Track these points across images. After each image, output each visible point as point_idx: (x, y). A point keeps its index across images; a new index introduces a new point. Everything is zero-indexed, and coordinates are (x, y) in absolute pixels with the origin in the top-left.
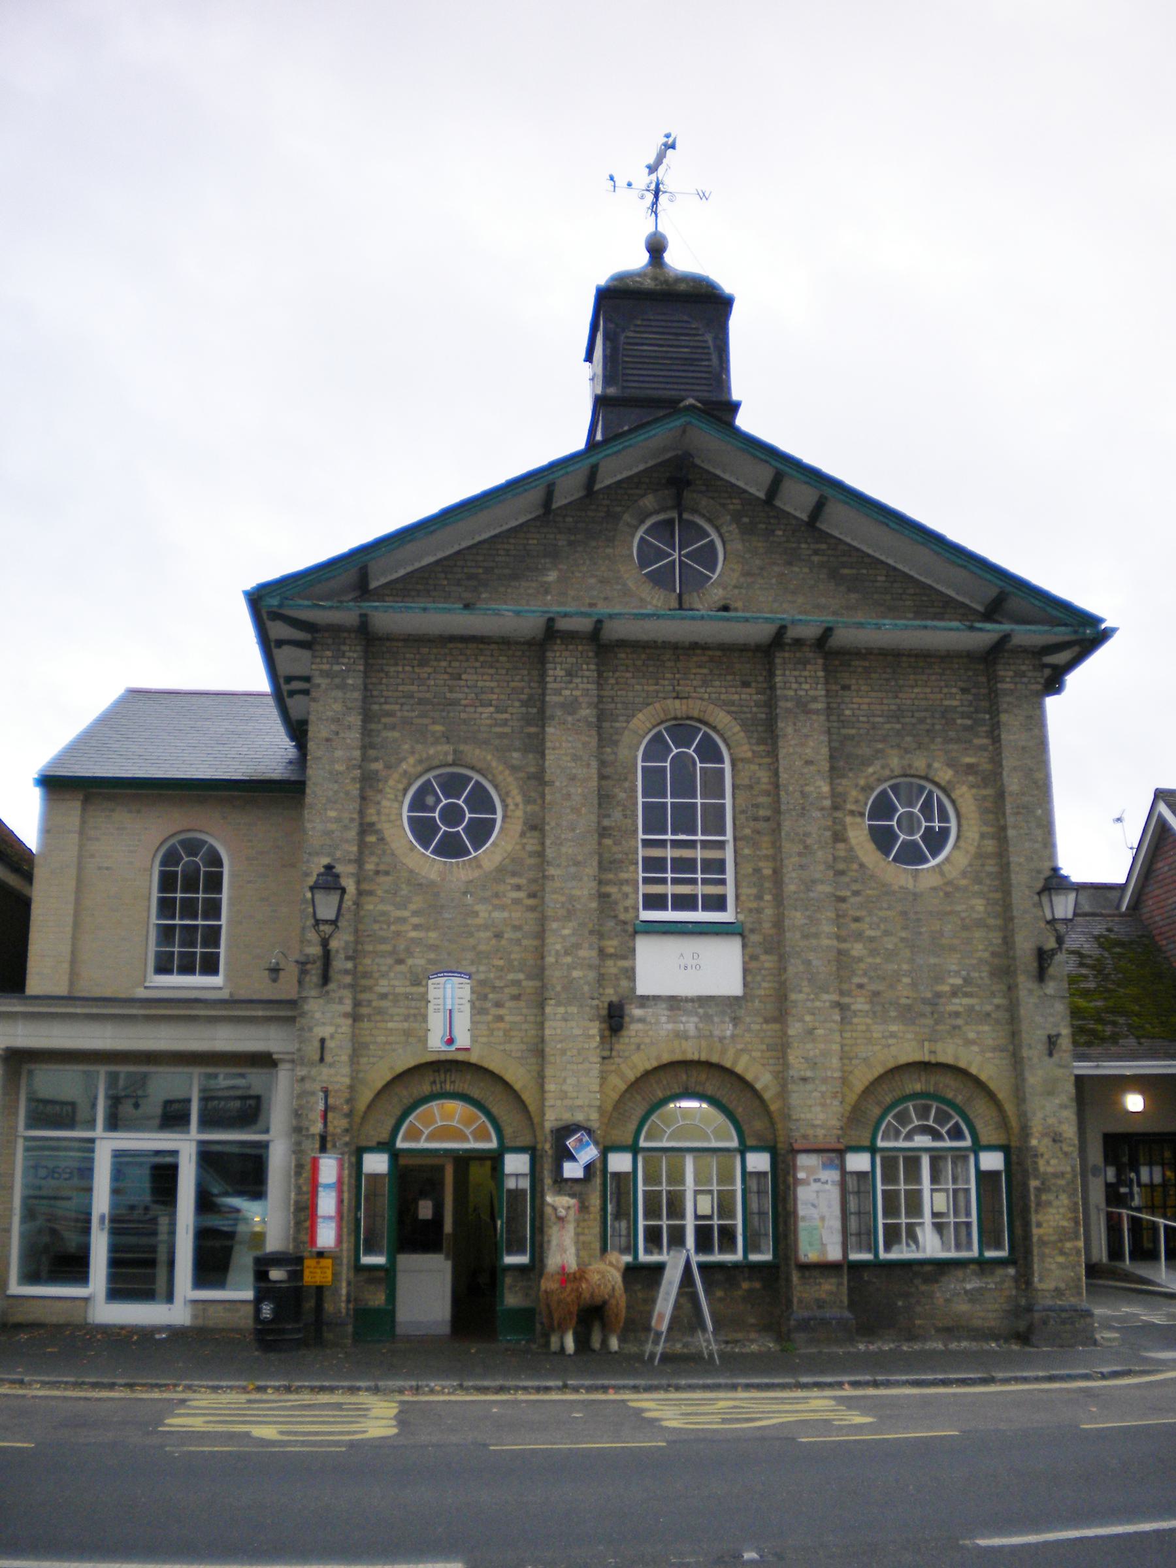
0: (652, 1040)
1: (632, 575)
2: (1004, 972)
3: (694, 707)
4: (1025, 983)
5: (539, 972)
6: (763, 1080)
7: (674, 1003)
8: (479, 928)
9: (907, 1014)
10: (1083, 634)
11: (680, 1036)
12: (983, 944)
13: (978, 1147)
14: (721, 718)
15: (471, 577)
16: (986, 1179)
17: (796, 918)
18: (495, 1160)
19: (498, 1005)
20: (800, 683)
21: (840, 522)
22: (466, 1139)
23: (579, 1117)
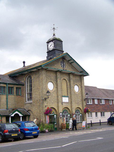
0: (65, 105)
1: (60, 66)
2: (82, 100)
3: (64, 78)
4: (84, 101)
5: (58, 100)
6: (70, 109)
7: (65, 102)
8: (53, 96)
9: (77, 104)
10: (87, 74)
11: (65, 105)
12: (81, 98)
13: (80, 114)
14: (66, 79)
15: (51, 65)
16: (80, 116)
17: (72, 96)
18: (54, 115)
19: (55, 103)
20: (71, 76)
21: (74, 64)
22: (51, 114)
23: (61, 112)
